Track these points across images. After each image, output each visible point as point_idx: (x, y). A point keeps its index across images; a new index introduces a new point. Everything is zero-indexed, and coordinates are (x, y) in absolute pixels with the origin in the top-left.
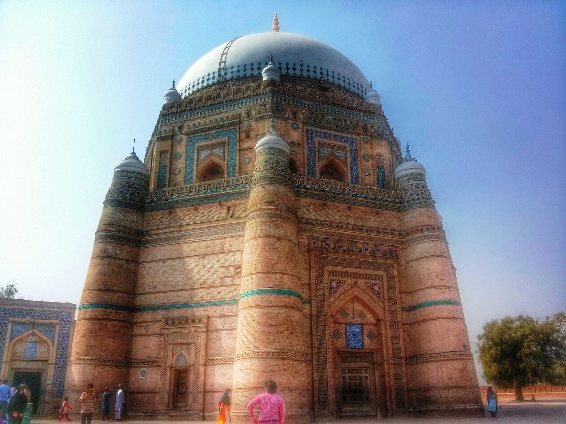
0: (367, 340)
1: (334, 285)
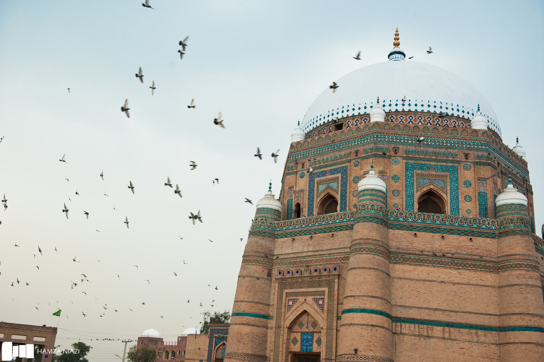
0: (315, 345)
1: (291, 303)
